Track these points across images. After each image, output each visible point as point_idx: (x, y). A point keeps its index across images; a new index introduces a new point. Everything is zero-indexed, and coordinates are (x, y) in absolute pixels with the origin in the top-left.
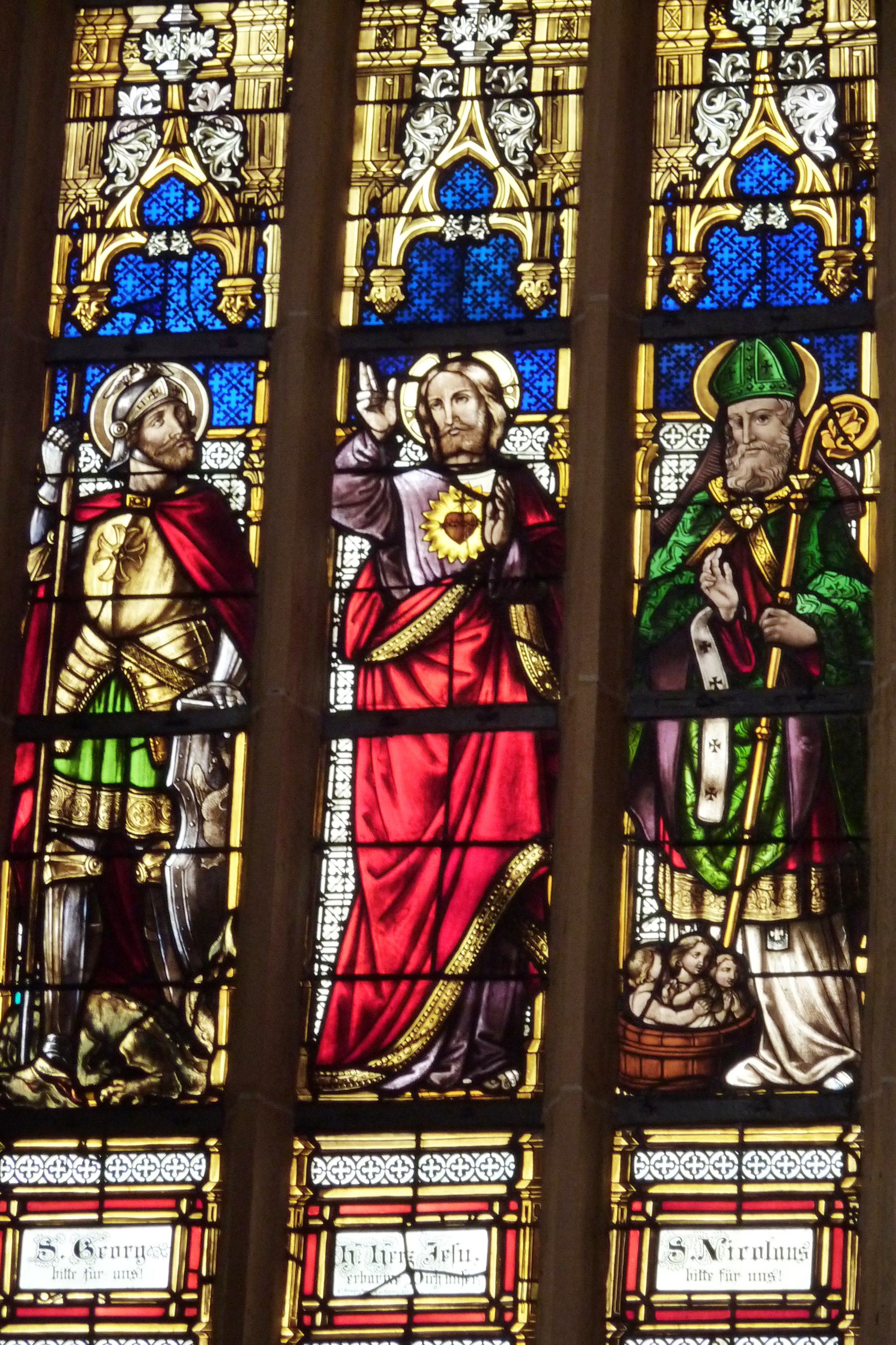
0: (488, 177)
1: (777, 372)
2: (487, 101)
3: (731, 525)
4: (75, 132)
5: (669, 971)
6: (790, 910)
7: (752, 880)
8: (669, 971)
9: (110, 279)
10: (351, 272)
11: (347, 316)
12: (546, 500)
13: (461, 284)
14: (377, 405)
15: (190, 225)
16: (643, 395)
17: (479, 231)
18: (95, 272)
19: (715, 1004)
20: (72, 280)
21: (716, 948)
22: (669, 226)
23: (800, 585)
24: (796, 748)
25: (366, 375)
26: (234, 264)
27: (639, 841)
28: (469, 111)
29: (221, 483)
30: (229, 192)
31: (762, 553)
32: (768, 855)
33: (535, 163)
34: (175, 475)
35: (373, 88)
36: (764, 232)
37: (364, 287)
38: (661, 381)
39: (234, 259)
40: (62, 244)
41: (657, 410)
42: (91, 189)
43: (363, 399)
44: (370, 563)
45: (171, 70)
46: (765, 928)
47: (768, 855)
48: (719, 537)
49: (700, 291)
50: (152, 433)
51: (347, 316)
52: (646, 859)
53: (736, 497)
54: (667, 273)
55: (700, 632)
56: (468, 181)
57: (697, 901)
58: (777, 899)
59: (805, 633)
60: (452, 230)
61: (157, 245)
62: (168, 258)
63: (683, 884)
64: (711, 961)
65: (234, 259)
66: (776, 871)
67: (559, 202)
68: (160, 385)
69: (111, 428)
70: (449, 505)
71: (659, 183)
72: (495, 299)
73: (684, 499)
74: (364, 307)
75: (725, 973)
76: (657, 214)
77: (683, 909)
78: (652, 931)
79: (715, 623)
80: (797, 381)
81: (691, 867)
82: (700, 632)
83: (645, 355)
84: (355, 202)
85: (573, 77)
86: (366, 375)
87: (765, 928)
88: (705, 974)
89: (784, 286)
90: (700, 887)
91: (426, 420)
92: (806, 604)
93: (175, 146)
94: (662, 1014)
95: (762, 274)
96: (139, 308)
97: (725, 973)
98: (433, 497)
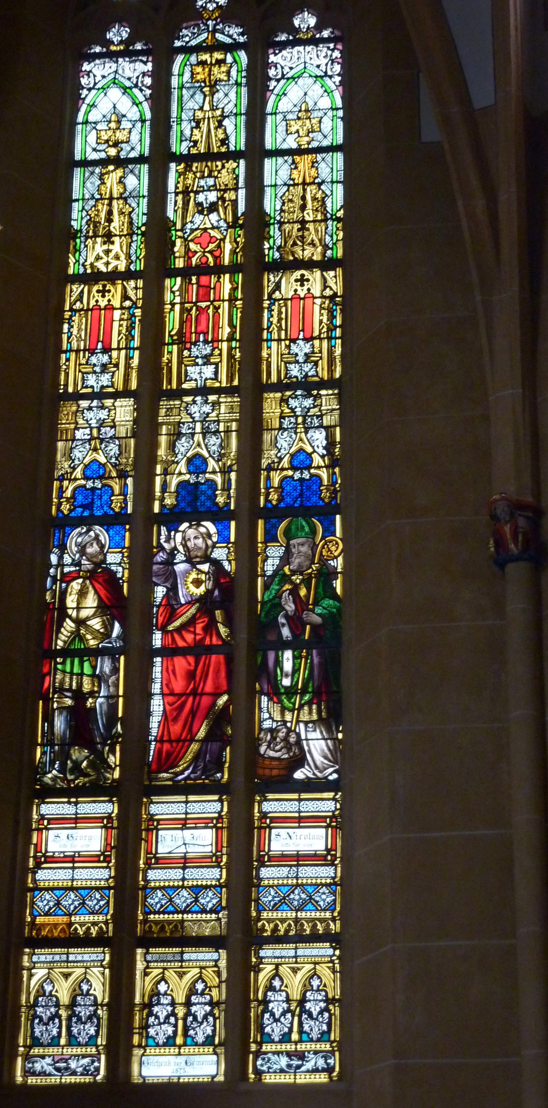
0: (205, 461)
1: (307, 529)
2: (204, 434)
3: (292, 582)
4: (60, 445)
5: (274, 738)
6: (315, 717)
7: (301, 706)
8: (274, 738)
9: (73, 496)
10: (158, 494)
11: (156, 509)
12: (227, 574)
13: (196, 498)
14: (168, 540)
15: (101, 477)
16: (260, 537)
17: (201, 479)
18: (68, 494)
19: (289, 750)
20: (60, 497)
21: (289, 730)
22: (268, 478)
23: (316, 603)
24: (316, 660)
25: (164, 530)
26: (117, 491)
27: (262, 693)
28: (198, 437)
29: (114, 568)
30: (115, 466)
31: (303, 592)
32: (307, 698)
33: (221, 456)
34: (97, 565)
35: (164, 430)
36: (301, 480)
37: (162, 499)
38: (267, 532)
39: (117, 489)
40: (56, 484)
41: (265, 542)
42: (66, 465)
43: (163, 538)
44: (166, 596)
45: (94, 423)
46: (306, 723)
47: (307, 698)
48: (287, 587)
49: (279, 500)
50: (89, 550)
51: (156, 509)
52: (264, 699)
53: (293, 572)
54: (268, 494)
55: (282, 620)
56: (198, 462)
57: (283, 714)
58: (310, 713)
59: (318, 620)
60: (192, 479)
61: (90, 484)
62: (93, 489)
63: (277, 708)
64: (288, 735)
65: (117, 489)
66: (310, 703)
67: (230, 470)
68: (92, 533)
69: (75, 549)
70: (193, 575)
71: (264, 463)
72: (208, 504)
73: (275, 573)
74: (162, 506)
75: (292, 739)
76: (264, 474)
77: (277, 717)
78: (267, 724)
79: (287, 616)
80: (314, 531)
81: (280, 702)
82: (282, 620)
83: (261, 523)
84: (159, 469)
85: (234, 426)
86: (164, 530)
87: (306, 723)
88: (286, 739)
89: (309, 499)
90: (283, 709)
91: (185, 546)
92: (318, 610)
93: (95, 450)
94: (272, 754)
95: (301, 495)
96: (84, 507)
97: (292, 739)
98: (187, 573)
